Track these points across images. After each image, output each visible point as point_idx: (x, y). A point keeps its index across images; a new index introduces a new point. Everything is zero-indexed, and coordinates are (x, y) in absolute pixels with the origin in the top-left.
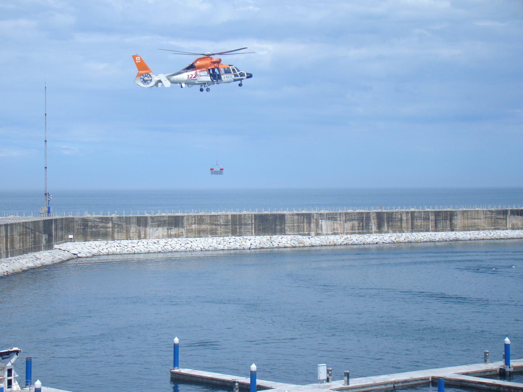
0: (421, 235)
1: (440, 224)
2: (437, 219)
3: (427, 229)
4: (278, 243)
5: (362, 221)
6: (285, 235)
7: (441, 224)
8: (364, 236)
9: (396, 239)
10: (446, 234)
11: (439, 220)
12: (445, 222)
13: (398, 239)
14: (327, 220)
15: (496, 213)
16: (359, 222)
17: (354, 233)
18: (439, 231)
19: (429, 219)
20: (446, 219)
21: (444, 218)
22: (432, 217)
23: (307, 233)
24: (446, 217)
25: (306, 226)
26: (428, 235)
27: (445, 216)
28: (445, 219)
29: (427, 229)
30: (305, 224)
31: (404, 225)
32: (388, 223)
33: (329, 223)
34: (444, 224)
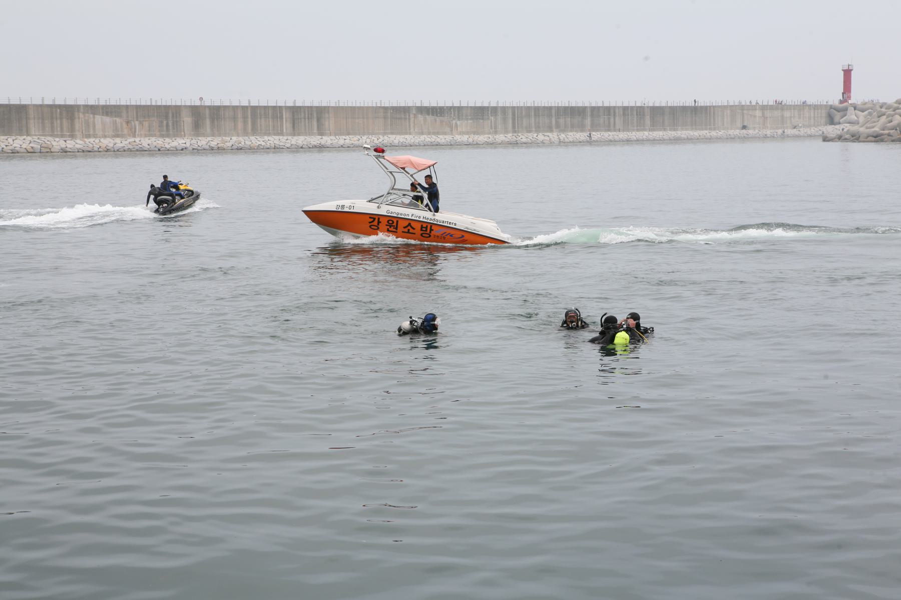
0: (263, 140)
1: (300, 124)
2: (295, 117)
3: (279, 132)
4: (5, 147)
5: (167, 117)
6: (28, 135)
7: (303, 124)
8: (164, 140)
9: (218, 144)
10: (306, 139)
11: (298, 118)
12: (309, 122)
13: (223, 145)
14: (103, 115)
15: (393, 110)
16: (160, 120)
17: (152, 136)
18: (299, 135)
19: (281, 117)
20: (311, 118)
21: (307, 116)
22: (286, 115)
23: (68, 134)
24: (310, 116)
25: (65, 123)
26: (275, 139)
27: (308, 115)
28: (308, 119)
29: (279, 132)
30: (64, 121)
31: (240, 125)
32: (212, 122)
33: (107, 119)
34: (307, 124)
